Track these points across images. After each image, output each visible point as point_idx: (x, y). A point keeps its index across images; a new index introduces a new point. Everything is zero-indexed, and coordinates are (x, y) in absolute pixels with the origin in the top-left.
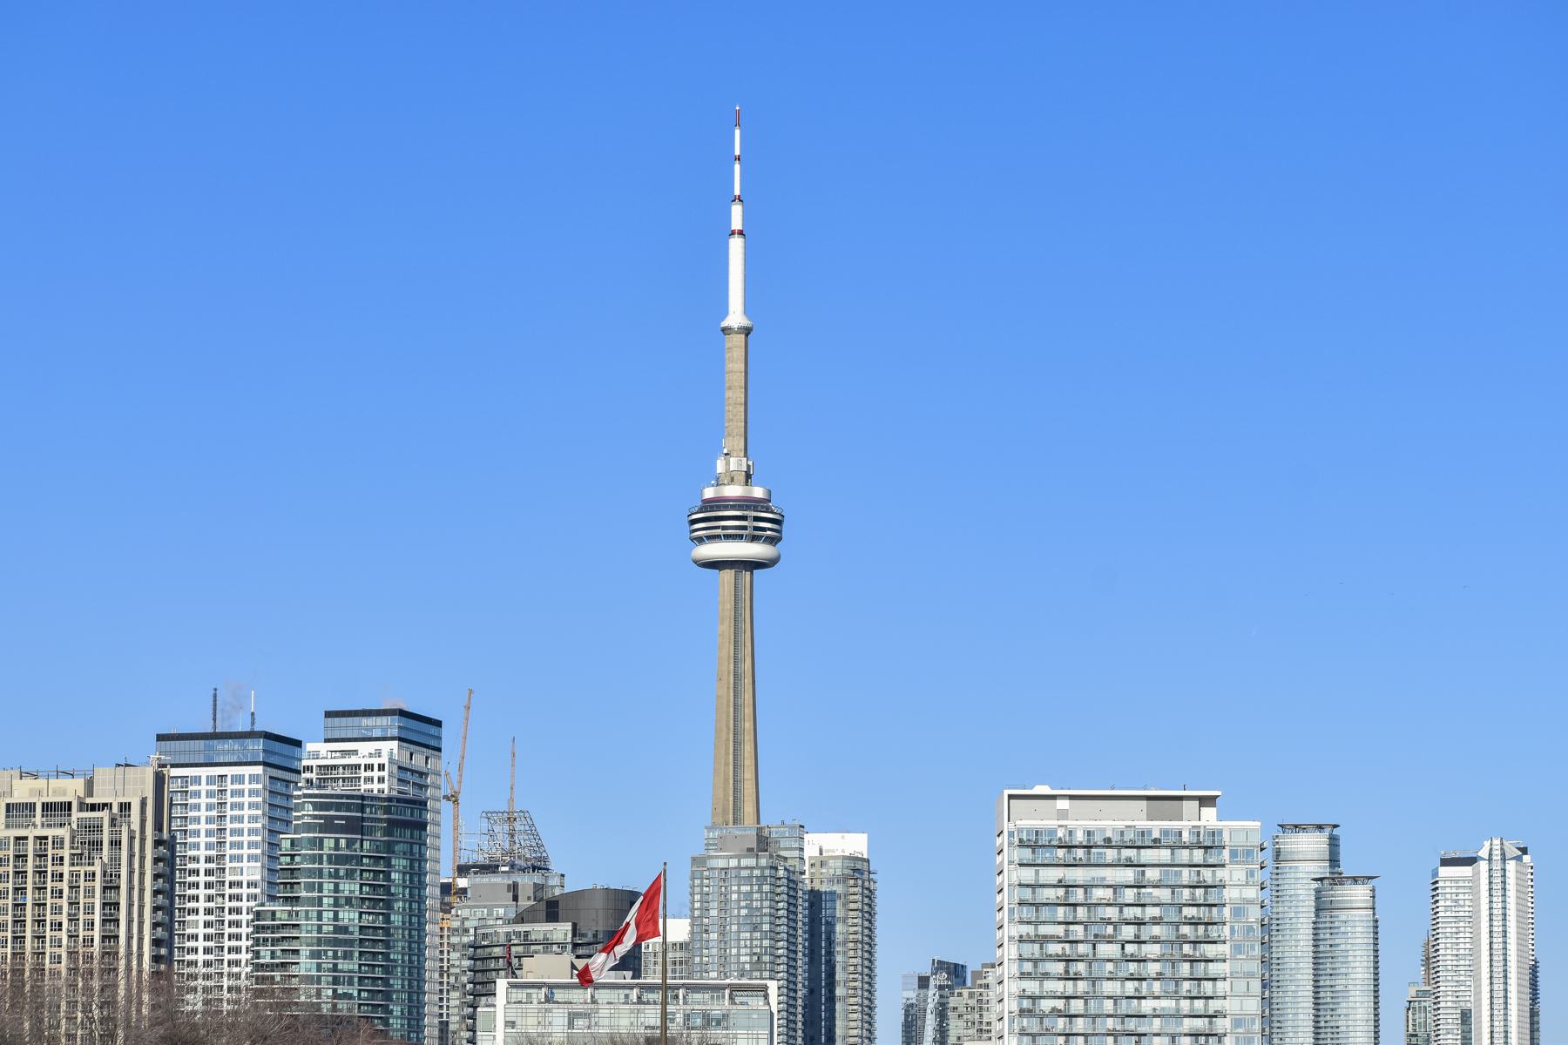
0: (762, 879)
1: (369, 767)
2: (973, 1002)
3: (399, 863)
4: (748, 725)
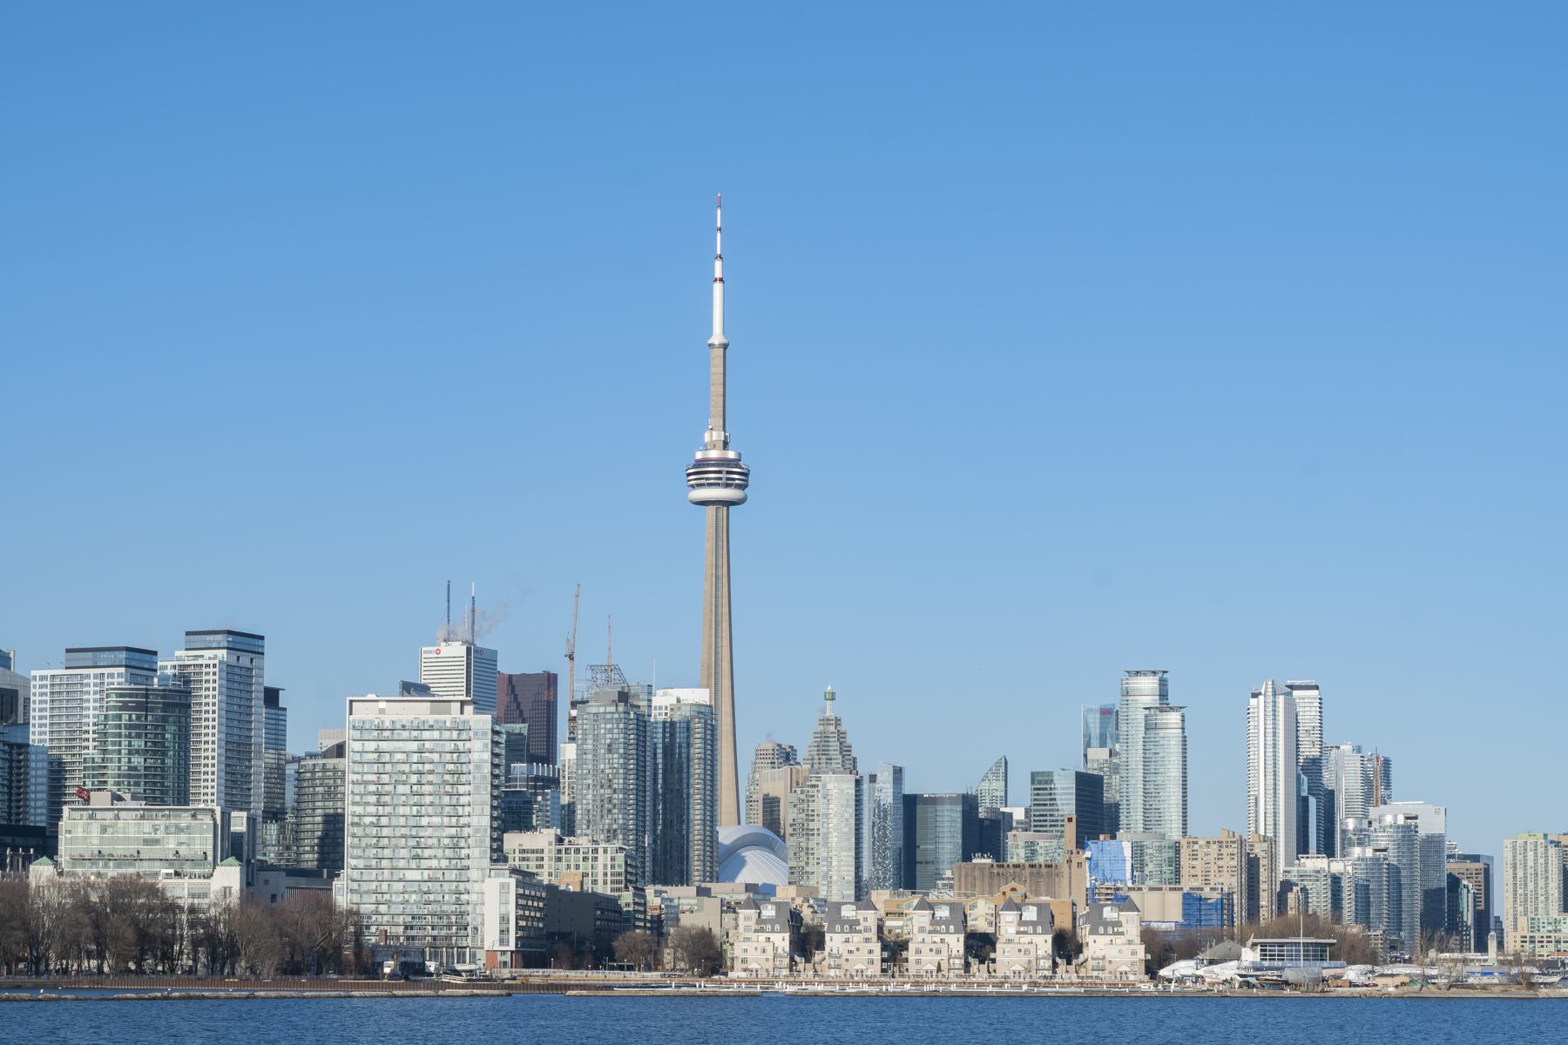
0: (619, 721)
1: (208, 666)
3: (171, 728)
4: (725, 610)
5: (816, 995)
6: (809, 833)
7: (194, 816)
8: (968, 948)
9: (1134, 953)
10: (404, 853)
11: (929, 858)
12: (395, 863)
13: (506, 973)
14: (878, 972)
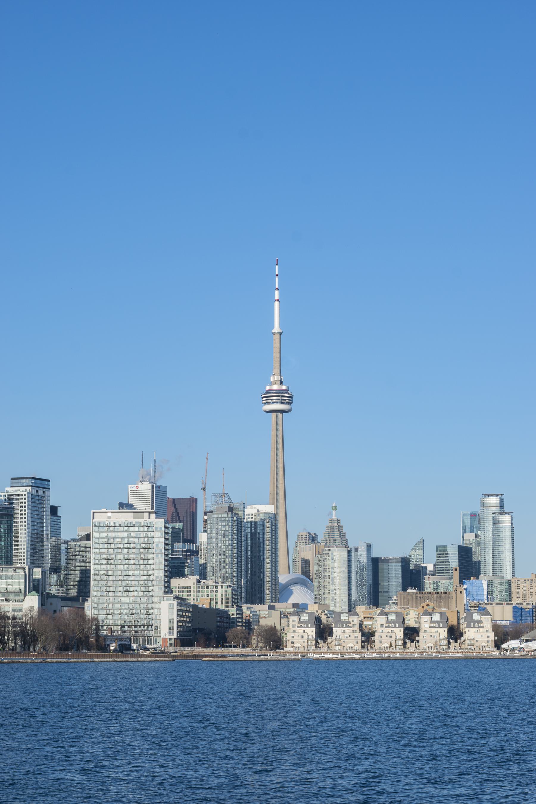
0: (228, 521)
1: (22, 495)
2: (321, 559)
4: (282, 465)
5: (329, 659)
6: (324, 578)
7: (15, 571)
8: (405, 635)
9: (489, 637)
10: (120, 589)
11: (385, 590)
12: (116, 594)
13: (172, 649)
14: (360, 648)
